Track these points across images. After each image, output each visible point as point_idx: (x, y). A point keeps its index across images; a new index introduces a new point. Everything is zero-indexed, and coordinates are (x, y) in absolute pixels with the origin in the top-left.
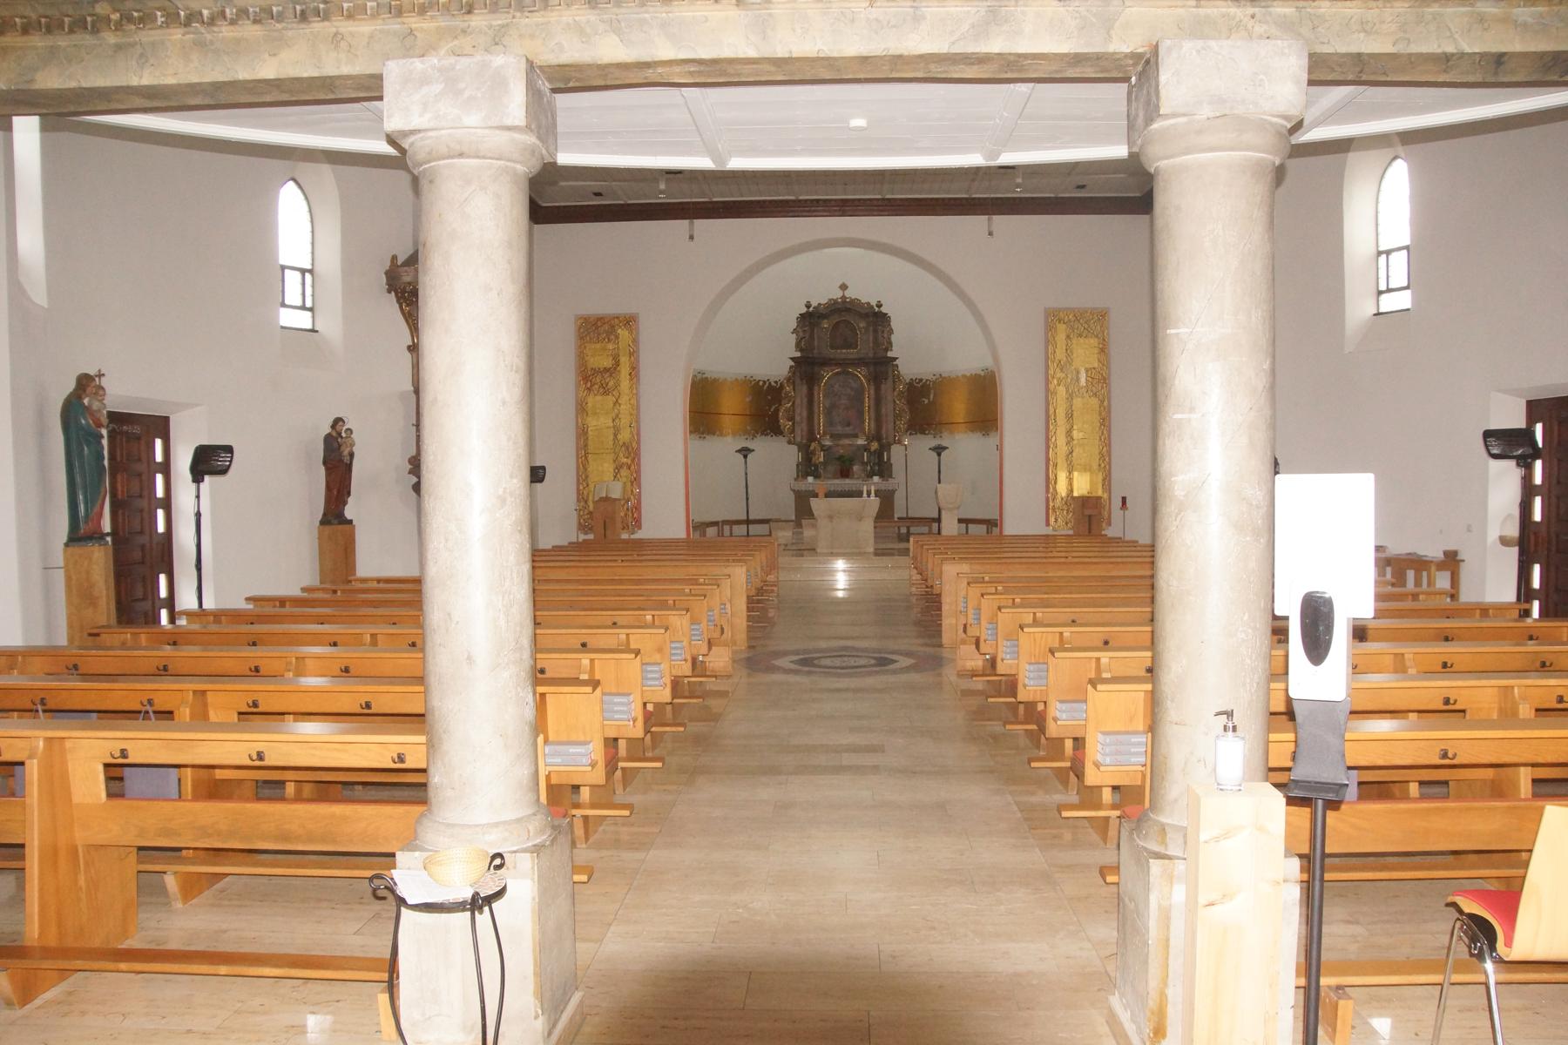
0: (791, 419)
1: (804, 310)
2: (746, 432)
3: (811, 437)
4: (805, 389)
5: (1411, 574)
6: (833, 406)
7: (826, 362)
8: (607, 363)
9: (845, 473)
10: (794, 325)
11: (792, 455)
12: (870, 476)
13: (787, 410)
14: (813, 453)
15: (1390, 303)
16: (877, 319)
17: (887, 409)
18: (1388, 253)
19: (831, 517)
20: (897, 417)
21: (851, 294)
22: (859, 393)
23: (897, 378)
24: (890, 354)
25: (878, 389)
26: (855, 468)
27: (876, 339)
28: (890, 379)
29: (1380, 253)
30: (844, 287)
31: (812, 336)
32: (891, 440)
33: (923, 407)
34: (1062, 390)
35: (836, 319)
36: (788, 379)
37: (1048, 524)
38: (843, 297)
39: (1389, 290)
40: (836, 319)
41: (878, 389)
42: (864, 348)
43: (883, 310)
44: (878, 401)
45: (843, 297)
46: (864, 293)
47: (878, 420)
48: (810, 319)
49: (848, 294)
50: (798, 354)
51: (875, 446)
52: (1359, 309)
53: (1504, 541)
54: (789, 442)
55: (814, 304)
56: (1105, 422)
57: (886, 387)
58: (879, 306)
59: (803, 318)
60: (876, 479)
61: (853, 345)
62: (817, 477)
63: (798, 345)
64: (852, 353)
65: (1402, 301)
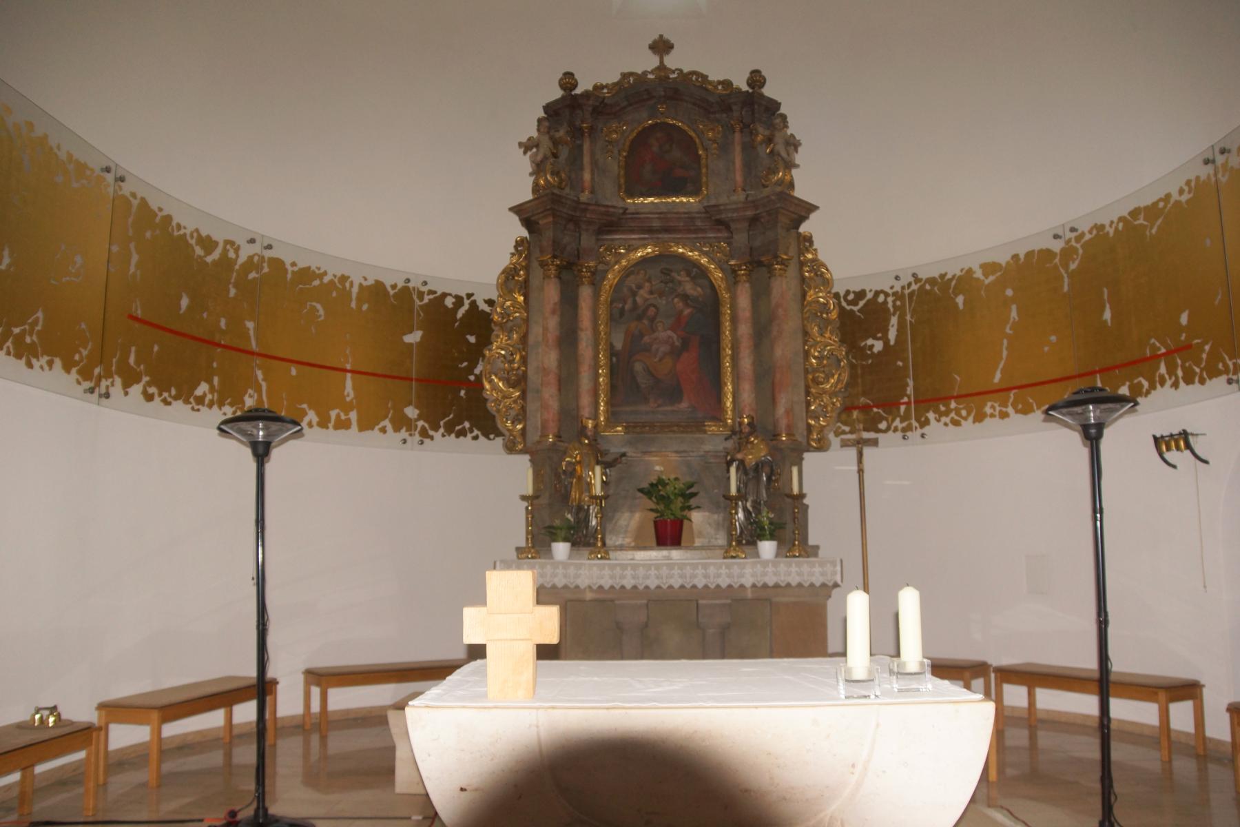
0: (519, 381)
1: (558, 94)
2: (401, 423)
4: (551, 293)
6: (635, 345)
7: (612, 223)
9: (669, 534)
11: (518, 474)
12: (748, 539)
17: (785, 349)
22: (710, 309)
25: (760, 294)
26: (697, 518)
28: (792, 271)
32: (800, 438)
36: (509, 275)
38: (662, 67)
41: (760, 294)
44: (763, 331)
45: (662, 67)
47: (766, 380)
49: (672, 61)
54: (510, 448)
57: (783, 286)
58: (757, 79)
59: (552, 111)
60: (767, 548)
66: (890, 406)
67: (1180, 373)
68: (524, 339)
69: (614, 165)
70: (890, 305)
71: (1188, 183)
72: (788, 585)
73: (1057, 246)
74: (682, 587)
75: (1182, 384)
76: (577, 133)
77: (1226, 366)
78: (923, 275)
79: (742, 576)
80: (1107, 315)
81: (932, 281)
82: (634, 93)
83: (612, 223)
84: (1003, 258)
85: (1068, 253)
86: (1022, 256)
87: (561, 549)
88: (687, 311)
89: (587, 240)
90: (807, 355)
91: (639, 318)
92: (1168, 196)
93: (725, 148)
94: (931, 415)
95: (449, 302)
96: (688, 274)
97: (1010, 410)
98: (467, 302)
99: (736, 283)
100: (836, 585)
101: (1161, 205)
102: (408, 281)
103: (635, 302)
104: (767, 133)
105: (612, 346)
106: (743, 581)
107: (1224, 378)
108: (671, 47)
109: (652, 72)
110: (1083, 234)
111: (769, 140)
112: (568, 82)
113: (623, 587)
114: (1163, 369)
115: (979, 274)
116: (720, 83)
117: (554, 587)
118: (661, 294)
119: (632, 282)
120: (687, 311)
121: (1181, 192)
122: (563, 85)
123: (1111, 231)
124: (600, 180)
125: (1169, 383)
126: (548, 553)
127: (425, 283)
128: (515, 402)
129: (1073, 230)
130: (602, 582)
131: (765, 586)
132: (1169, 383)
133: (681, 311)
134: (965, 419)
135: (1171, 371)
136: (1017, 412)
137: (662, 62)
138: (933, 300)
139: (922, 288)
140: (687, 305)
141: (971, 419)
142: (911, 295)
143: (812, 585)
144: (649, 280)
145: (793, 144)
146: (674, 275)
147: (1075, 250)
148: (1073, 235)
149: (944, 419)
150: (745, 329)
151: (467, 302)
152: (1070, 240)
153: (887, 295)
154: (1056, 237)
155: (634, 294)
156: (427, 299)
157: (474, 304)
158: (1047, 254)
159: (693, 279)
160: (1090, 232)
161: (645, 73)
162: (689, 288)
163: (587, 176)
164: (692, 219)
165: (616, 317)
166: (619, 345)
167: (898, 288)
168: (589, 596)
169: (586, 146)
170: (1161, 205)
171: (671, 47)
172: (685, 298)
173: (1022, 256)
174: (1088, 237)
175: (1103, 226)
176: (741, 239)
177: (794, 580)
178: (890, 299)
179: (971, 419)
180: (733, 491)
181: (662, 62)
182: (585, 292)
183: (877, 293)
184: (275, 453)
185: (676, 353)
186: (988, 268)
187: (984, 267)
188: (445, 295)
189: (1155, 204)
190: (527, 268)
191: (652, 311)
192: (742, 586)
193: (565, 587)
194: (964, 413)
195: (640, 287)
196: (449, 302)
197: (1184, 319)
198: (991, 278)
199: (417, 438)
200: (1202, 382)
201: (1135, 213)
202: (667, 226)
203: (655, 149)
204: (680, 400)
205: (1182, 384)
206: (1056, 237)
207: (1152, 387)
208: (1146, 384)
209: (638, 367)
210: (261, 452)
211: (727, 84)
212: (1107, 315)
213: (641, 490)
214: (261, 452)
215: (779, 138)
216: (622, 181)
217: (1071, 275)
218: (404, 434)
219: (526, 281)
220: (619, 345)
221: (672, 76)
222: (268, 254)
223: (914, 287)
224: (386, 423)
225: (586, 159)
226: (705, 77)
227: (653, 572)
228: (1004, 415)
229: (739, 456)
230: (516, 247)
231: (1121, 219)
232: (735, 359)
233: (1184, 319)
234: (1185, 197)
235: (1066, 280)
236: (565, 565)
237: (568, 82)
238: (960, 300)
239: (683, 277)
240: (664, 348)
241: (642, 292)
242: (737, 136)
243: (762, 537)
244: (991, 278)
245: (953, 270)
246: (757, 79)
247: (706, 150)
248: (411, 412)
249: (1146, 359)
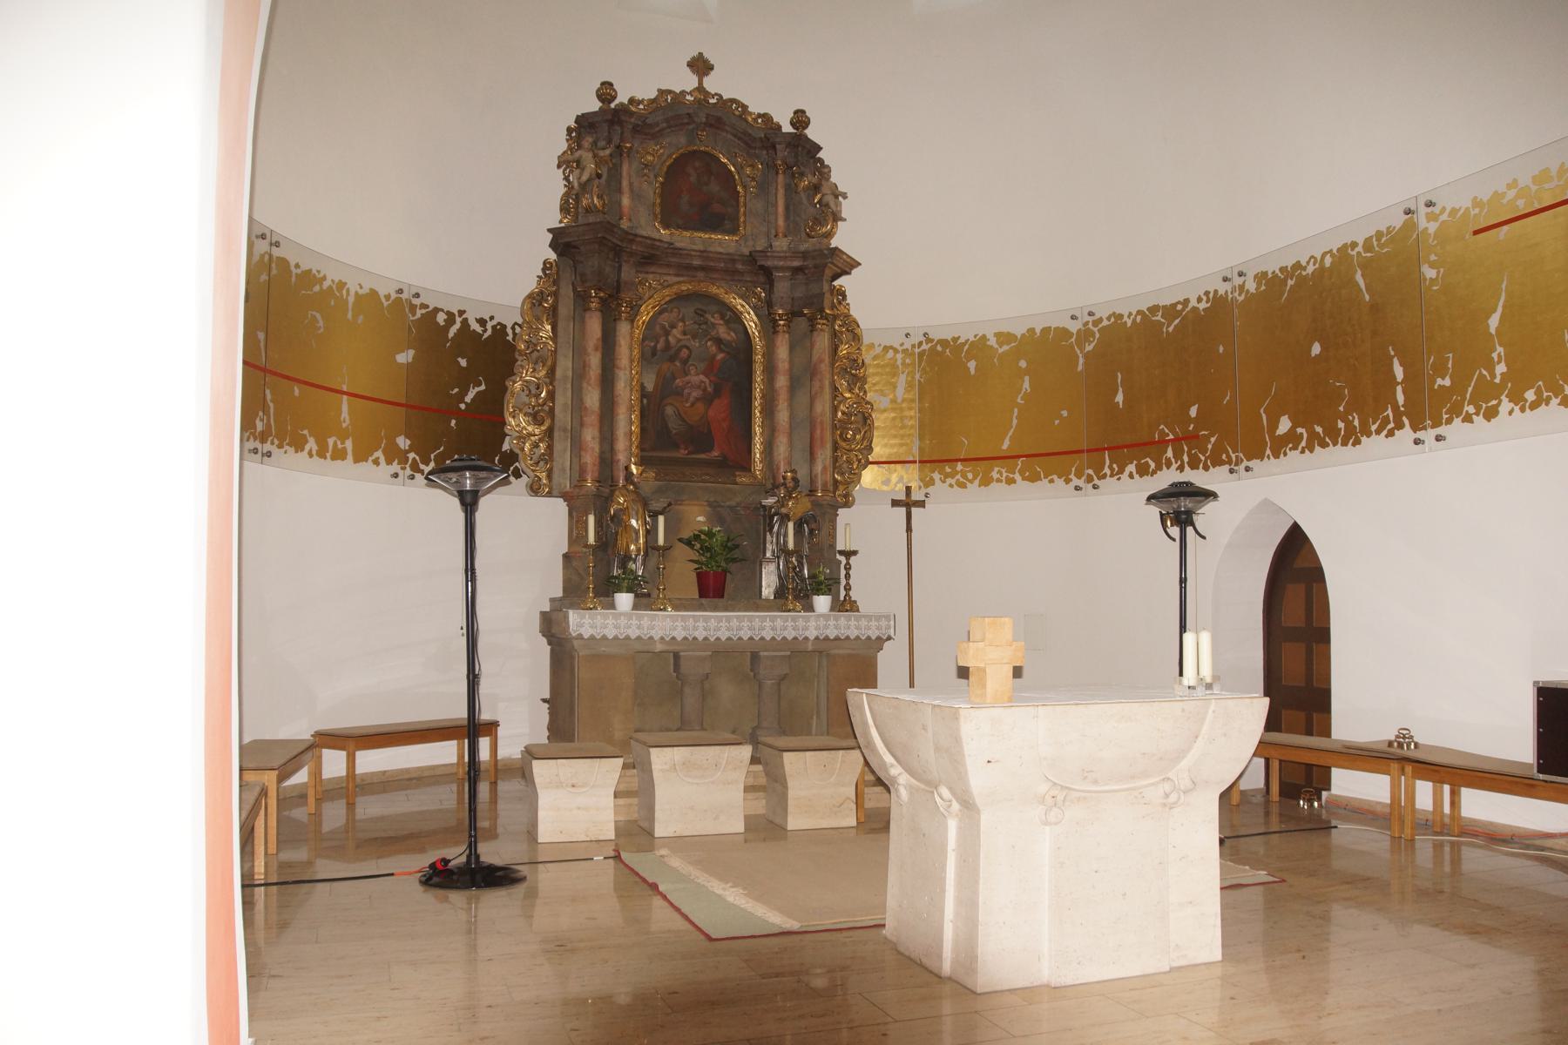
1: (594, 105)
2: (394, 454)
4: (594, 326)
13: (532, 390)
14: (619, 519)
30: (700, 66)
36: (535, 300)
42: (761, 228)
45: (700, 88)
49: (710, 84)
51: (798, 506)
54: (534, 489)
55: (622, 98)
58: (800, 120)
60: (822, 602)
61: (716, 217)
67: (1186, 458)
68: (552, 373)
69: (651, 190)
70: (899, 362)
71: (1207, 293)
72: (848, 638)
73: (1074, 327)
74: (751, 638)
75: (1187, 468)
77: (1229, 456)
78: (936, 335)
79: (806, 628)
80: (1120, 398)
81: (944, 343)
82: (671, 114)
83: (652, 256)
84: (1019, 331)
85: (1085, 335)
86: (1038, 331)
87: (624, 600)
88: (720, 356)
89: (628, 273)
90: (835, 409)
91: (672, 359)
92: (1187, 301)
93: (764, 188)
94: (936, 476)
95: (441, 318)
96: (722, 318)
97: (1017, 477)
98: (458, 320)
99: (775, 332)
100: (889, 638)
101: (1179, 307)
102: (400, 291)
103: (667, 341)
104: (815, 180)
105: (643, 387)
106: (807, 634)
107: (1227, 467)
108: (711, 68)
109: (690, 93)
110: (1101, 320)
111: (816, 188)
112: (606, 92)
113: (695, 638)
114: (1170, 453)
115: (992, 342)
116: (760, 116)
117: (628, 638)
118: (694, 337)
119: (665, 319)
120: (720, 356)
121: (1199, 300)
122: (600, 96)
123: (1129, 323)
124: (638, 211)
125: (1175, 466)
126: (612, 606)
127: (417, 295)
128: (541, 440)
129: (1091, 314)
130: (675, 634)
131: (827, 638)
132: (1175, 466)
133: (714, 357)
134: (971, 482)
135: (1178, 455)
136: (1024, 479)
137: (700, 83)
139: (933, 349)
140: (721, 350)
141: (977, 482)
142: (921, 354)
143: (869, 638)
144: (683, 320)
145: (837, 194)
146: (708, 316)
147: (1093, 334)
148: (1091, 319)
149: (949, 481)
150: (782, 382)
151: (458, 320)
152: (1086, 323)
153: (896, 351)
154: (1073, 317)
155: (667, 333)
156: (419, 313)
157: (465, 322)
158: (1064, 333)
159: (727, 322)
160: (1109, 319)
161: (683, 93)
162: (722, 332)
163: (626, 201)
164: (734, 261)
165: (649, 356)
166: (650, 387)
167: (908, 346)
168: (659, 647)
169: (625, 167)
170: (1179, 307)
171: (711, 68)
172: (719, 341)
173: (1038, 331)
174: (1105, 323)
175: (1121, 316)
177: (853, 633)
178: (899, 356)
179: (977, 482)
180: (791, 545)
181: (700, 83)
182: (623, 328)
183: (886, 349)
184: (484, 502)
185: (708, 399)
187: (998, 335)
188: (437, 310)
189: (1174, 305)
190: (555, 294)
191: (684, 353)
192: (806, 638)
193: (639, 638)
194: (970, 476)
195: (673, 326)
196: (441, 318)
197: (1193, 412)
198: (1005, 348)
199: (408, 472)
200: (1206, 468)
201: (1154, 309)
202: (709, 266)
203: (693, 179)
204: (710, 450)
205: (1187, 468)
206: (1073, 317)
207: (1159, 468)
208: (1153, 465)
209: (669, 410)
211: (766, 117)
212: (1120, 398)
213: (680, 540)
215: (825, 189)
216: (658, 210)
217: (1086, 356)
218: (395, 467)
219: (554, 308)
220: (650, 387)
221: (712, 101)
222: (276, 252)
223: (925, 347)
224: (379, 454)
225: (625, 183)
226: (745, 107)
227: (874, 623)
228: (1010, 481)
229: (784, 510)
230: (543, 270)
231: (1139, 312)
232: (769, 411)
233: (1193, 412)
234: (1202, 306)
235: (1081, 361)
236: (628, 616)
237: (606, 92)
238: (972, 365)
239: (715, 319)
240: (695, 394)
241: (675, 331)
242: (781, 178)
243: (818, 592)
244: (1005, 348)
245: (967, 335)
246: (800, 120)
247: (744, 187)
248: (403, 442)
249: (1154, 443)
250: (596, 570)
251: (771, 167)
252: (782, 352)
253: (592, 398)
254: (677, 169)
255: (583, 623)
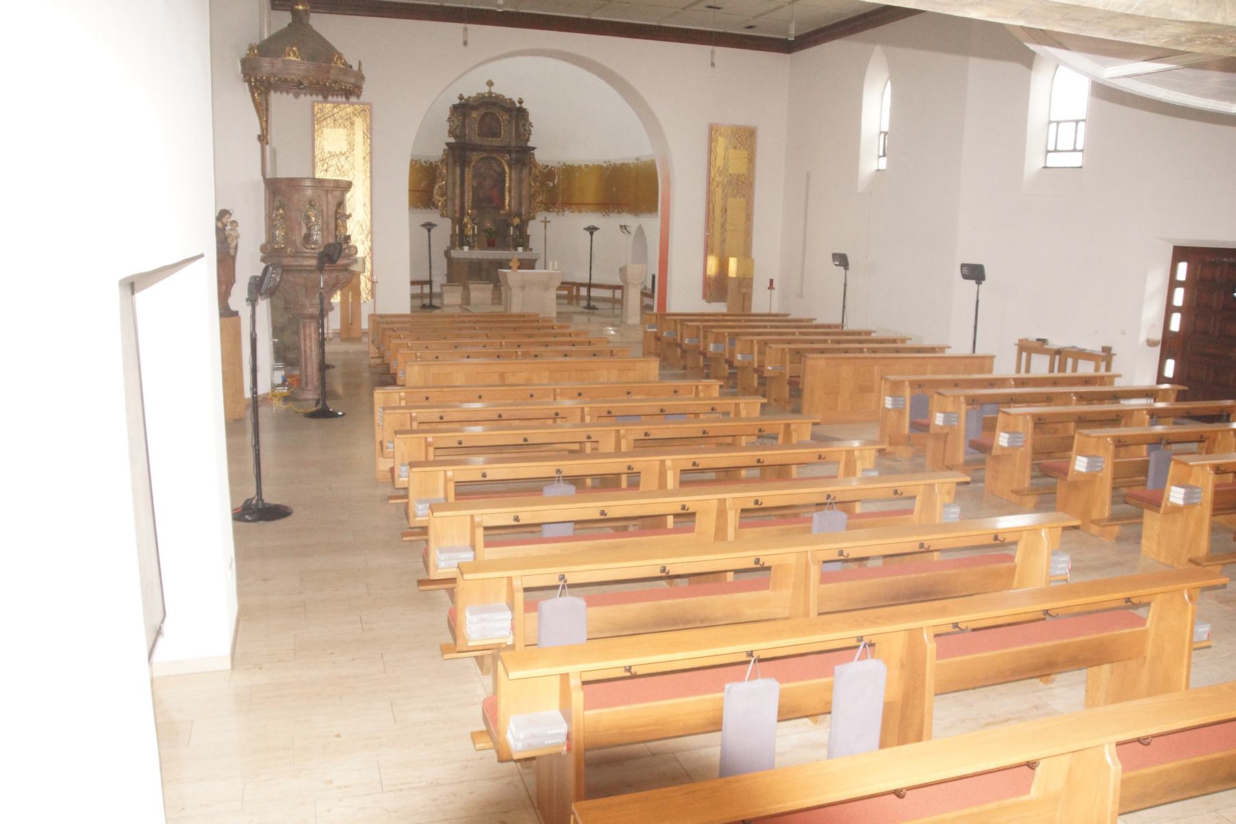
1: (457, 101)
3: (463, 212)
4: (458, 171)
5: (1070, 361)
8: (344, 147)
10: (447, 114)
13: (441, 188)
14: (466, 225)
15: (1054, 160)
16: (518, 114)
18: (1058, 123)
19: (523, 288)
20: (532, 197)
21: (496, 90)
23: (536, 165)
24: (530, 144)
27: (517, 129)
29: (1050, 122)
30: (490, 84)
31: (463, 126)
33: (558, 189)
34: (719, 190)
35: (483, 110)
36: (442, 161)
37: (704, 297)
38: (490, 93)
39: (1056, 151)
40: (483, 110)
42: (506, 137)
43: (524, 106)
45: (490, 93)
46: (508, 90)
48: (462, 109)
49: (494, 90)
50: (452, 140)
51: (517, 221)
52: (1034, 162)
53: (1151, 343)
54: (442, 215)
55: (466, 97)
56: (749, 218)
58: (521, 102)
60: (520, 249)
61: (495, 134)
62: (471, 248)
63: (451, 133)
64: (495, 142)
65: (1076, 160)
66: (554, 204)
76: (465, 115)
87: (466, 248)
112: (461, 98)
138: (569, 171)
165: (474, 176)
176: (514, 155)
186: (587, 166)
210: (429, 231)
214: (429, 231)
250: (460, 239)
251: (511, 116)
252: (513, 176)
253: (458, 191)
254: (483, 117)
255: (456, 254)
